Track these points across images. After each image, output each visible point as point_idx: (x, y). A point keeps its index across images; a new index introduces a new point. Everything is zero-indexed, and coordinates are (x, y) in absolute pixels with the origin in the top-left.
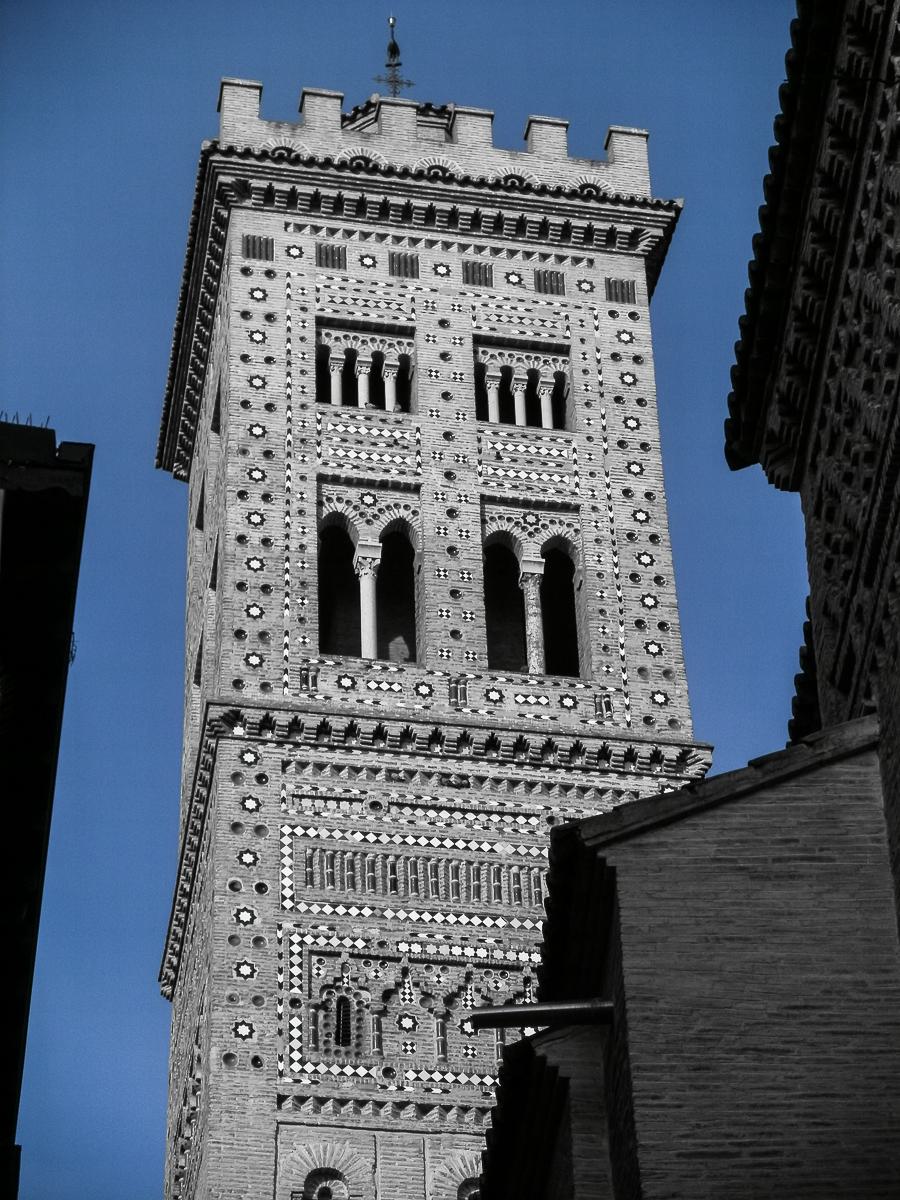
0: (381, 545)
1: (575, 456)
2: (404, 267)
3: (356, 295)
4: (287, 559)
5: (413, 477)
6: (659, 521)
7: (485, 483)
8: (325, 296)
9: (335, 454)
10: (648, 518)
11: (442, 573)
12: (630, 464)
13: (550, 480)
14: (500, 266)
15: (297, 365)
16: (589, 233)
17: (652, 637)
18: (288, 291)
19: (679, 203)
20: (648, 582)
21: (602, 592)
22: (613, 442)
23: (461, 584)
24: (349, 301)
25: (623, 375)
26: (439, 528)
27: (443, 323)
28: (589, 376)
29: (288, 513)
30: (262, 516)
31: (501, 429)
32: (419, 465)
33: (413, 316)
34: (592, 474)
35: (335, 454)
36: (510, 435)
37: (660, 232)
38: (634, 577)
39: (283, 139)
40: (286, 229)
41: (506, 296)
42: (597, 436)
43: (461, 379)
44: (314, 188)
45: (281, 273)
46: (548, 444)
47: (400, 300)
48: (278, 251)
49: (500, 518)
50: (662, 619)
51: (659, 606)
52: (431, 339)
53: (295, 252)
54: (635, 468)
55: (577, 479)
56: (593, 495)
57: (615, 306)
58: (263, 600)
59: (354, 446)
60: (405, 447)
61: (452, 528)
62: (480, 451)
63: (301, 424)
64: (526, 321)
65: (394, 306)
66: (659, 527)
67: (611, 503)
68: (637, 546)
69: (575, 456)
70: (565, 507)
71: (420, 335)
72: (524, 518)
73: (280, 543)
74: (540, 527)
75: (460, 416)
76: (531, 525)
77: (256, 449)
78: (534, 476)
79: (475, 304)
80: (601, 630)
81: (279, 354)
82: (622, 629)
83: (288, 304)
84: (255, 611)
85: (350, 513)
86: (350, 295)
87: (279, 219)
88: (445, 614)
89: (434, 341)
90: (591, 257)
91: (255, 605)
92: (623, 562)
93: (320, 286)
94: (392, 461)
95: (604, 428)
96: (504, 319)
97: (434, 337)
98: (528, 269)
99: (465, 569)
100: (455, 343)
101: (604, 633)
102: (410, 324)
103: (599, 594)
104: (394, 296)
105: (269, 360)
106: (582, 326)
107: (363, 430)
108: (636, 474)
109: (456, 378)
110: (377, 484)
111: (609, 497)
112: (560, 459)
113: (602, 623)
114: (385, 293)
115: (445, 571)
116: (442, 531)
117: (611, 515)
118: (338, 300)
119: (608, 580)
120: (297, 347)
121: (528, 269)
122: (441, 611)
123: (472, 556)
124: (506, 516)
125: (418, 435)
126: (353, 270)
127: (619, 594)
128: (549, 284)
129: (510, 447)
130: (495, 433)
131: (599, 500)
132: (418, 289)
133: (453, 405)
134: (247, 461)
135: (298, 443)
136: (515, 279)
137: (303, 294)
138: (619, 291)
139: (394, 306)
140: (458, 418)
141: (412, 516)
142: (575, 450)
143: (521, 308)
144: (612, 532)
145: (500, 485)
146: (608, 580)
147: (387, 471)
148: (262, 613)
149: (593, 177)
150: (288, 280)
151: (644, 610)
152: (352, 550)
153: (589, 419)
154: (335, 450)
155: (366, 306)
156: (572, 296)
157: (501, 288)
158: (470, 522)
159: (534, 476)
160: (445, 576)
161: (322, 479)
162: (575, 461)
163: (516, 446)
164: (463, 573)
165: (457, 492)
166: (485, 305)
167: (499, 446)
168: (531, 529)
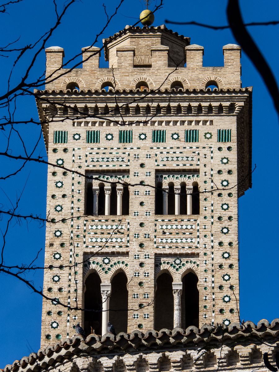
0: (110, 284)
1: (198, 228)
2: (125, 137)
3: (104, 156)
4: (69, 297)
5: (126, 249)
6: (234, 257)
7: (157, 247)
8: (89, 159)
9: (92, 241)
10: (229, 256)
11: (136, 296)
12: (223, 228)
13: (186, 242)
14: (170, 130)
15: (77, 196)
16: (210, 108)
17: (226, 317)
18: (73, 158)
19: (250, 89)
20: (226, 289)
21: (206, 297)
22: (216, 218)
23: (144, 301)
24: (100, 160)
25: (223, 181)
26: (136, 273)
27: (142, 165)
28: (207, 185)
29: (70, 274)
30: (59, 277)
31: (165, 218)
32: (128, 241)
33: (129, 164)
34: (205, 236)
35: (92, 241)
36: (170, 220)
37: (242, 104)
38: (221, 287)
39: (72, 78)
40: (74, 125)
41: (171, 146)
42: (209, 216)
43: (149, 194)
44: (85, 104)
45: (70, 150)
46: (186, 223)
47: (123, 156)
48: (70, 137)
49: (164, 263)
50: (232, 307)
51: (231, 300)
52: (136, 174)
53: (77, 137)
54: (225, 231)
55: (198, 240)
56: (205, 247)
57: (221, 145)
58: (58, 319)
59: (100, 236)
60: (123, 233)
61: (141, 273)
62: (156, 231)
63: (77, 227)
64: (180, 159)
65: (120, 159)
66: (234, 260)
67: (213, 250)
68: (223, 271)
69: (198, 228)
70: (193, 255)
71: (132, 173)
72: (175, 261)
73: (67, 290)
74: (181, 265)
75: (148, 214)
76: (178, 265)
77: (57, 242)
78: (179, 241)
79: (157, 153)
80: (204, 316)
81: (68, 193)
82: (213, 314)
83: (73, 165)
84: (55, 325)
85: (98, 269)
86: (101, 157)
87: (69, 122)
88: (136, 316)
89: (138, 175)
90: (211, 119)
91: (55, 322)
92: (216, 280)
93: (87, 153)
94: (116, 241)
95: (212, 211)
96: (170, 159)
97: (138, 173)
98: (181, 130)
99: (146, 293)
100: (147, 175)
101: (205, 317)
102: (127, 168)
103: (204, 298)
104: (120, 154)
105: (64, 196)
106: (205, 158)
107: (104, 227)
108: (225, 234)
109: (146, 194)
110: (110, 253)
111: (212, 247)
112: (191, 230)
113: (205, 312)
114: (117, 153)
115: (137, 295)
116: (137, 274)
117: (213, 256)
118: (95, 160)
119: (209, 290)
120: (76, 187)
121: (181, 130)
122: (135, 315)
123: (149, 286)
124: (167, 262)
125: (128, 226)
126: (103, 143)
127: (214, 297)
128: (192, 136)
129: (169, 227)
130: (163, 221)
131: (208, 249)
132: (132, 148)
133: (145, 208)
134: (53, 250)
135: (76, 238)
136: (175, 136)
137: (80, 159)
138: (223, 136)
139: (120, 159)
140: (147, 215)
141: (125, 267)
142: (198, 225)
143: (178, 151)
144: (213, 265)
145: (164, 247)
146: (209, 290)
147: (114, 247)
148: (58, 325)
149: (214, 76)
150: (74, 152)
151: (224, 303)
152: (101, 282)
153: (205, 207)
154: (91, 239)
155: (108, 161)
156: (202, 142)
157: (169, 142)
158: (149, 268)
159: (179, 241)
160: (137, 297)
161: (85, 254)
162: (198, 230)
163: (172, 226)
164: (145, 295)
165: (145, 253)
166: (161, 153)
167: (164, 227)
168: (177, 267)
